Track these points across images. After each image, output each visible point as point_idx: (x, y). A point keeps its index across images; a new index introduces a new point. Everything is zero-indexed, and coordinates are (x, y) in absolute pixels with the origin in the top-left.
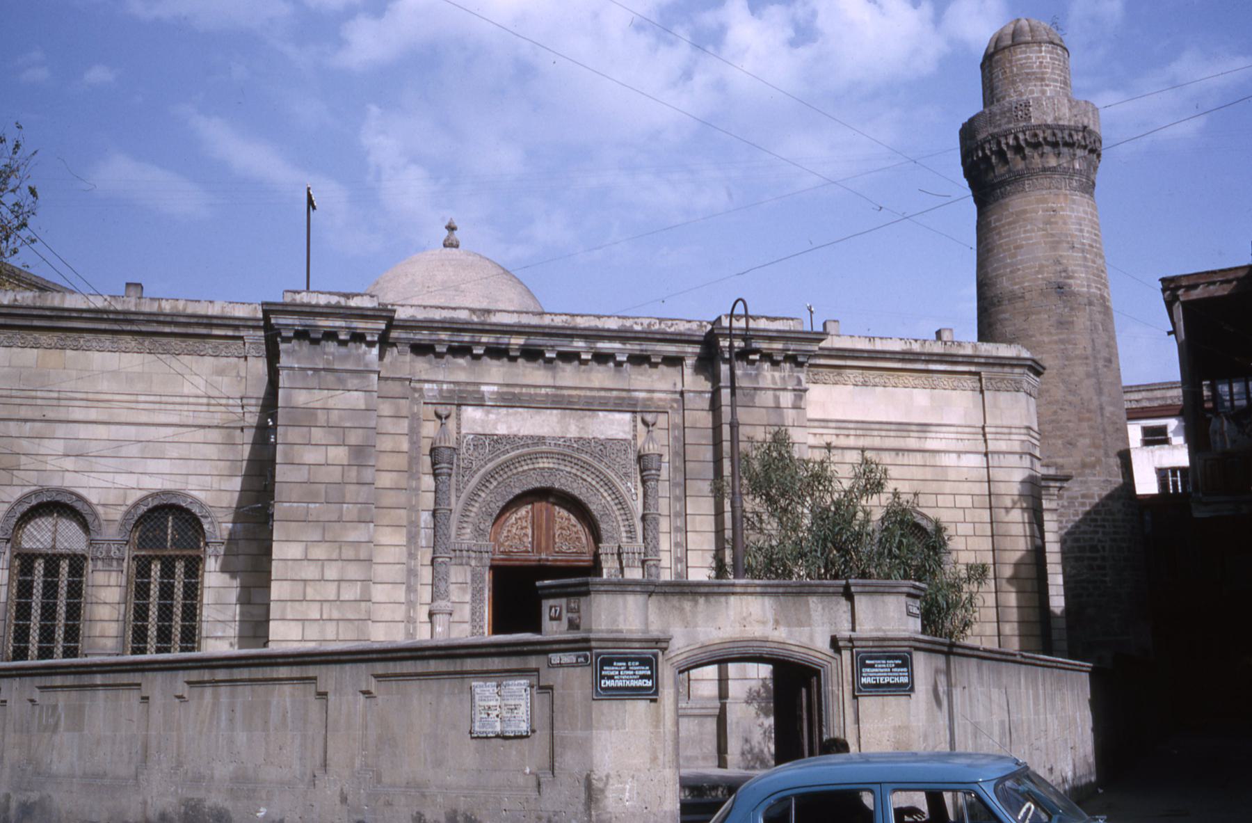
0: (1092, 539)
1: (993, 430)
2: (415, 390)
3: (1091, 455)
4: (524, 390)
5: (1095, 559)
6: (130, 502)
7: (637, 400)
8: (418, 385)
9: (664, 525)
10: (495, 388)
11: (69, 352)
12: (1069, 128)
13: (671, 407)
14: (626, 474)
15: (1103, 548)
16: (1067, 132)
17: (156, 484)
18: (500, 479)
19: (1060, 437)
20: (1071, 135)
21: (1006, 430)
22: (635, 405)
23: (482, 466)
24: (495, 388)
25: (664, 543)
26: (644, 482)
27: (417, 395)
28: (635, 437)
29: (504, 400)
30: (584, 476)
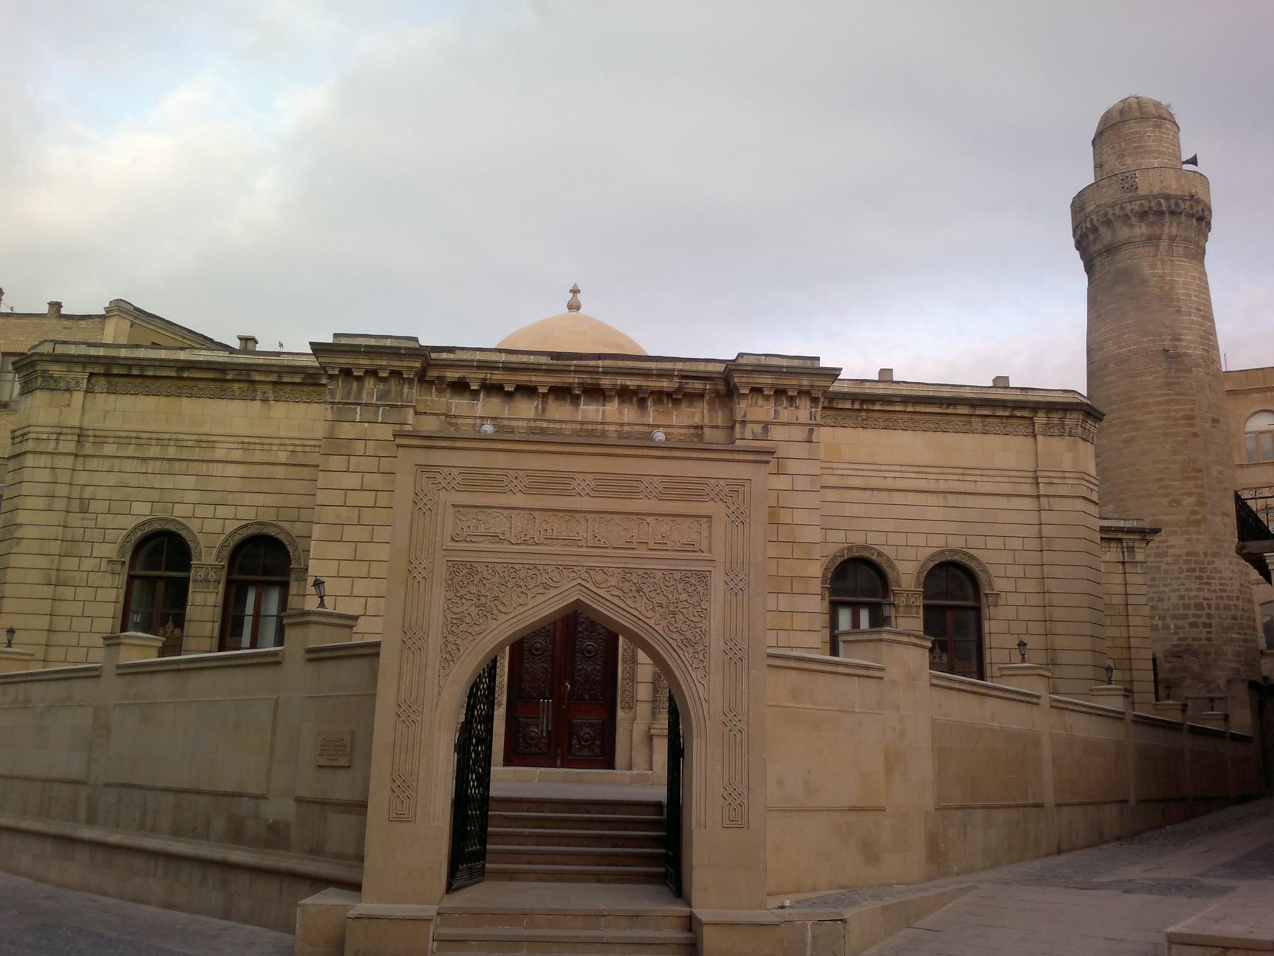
0: (1197, 597)
1: (1046, 474)
2: (451, 424)
3: (1195, 513)
4: (551, 425)
5: (1200, 616)
6: (228, 531)
8: (454, 421)
11: (185, 401)
12: (1175, 197)
15: (1209, 606)
16: (1173, 201)
17: (249, 515)
19: (1166, 495)
20: (1177, 204)
21: (1059, 474)
24: (525, 424)
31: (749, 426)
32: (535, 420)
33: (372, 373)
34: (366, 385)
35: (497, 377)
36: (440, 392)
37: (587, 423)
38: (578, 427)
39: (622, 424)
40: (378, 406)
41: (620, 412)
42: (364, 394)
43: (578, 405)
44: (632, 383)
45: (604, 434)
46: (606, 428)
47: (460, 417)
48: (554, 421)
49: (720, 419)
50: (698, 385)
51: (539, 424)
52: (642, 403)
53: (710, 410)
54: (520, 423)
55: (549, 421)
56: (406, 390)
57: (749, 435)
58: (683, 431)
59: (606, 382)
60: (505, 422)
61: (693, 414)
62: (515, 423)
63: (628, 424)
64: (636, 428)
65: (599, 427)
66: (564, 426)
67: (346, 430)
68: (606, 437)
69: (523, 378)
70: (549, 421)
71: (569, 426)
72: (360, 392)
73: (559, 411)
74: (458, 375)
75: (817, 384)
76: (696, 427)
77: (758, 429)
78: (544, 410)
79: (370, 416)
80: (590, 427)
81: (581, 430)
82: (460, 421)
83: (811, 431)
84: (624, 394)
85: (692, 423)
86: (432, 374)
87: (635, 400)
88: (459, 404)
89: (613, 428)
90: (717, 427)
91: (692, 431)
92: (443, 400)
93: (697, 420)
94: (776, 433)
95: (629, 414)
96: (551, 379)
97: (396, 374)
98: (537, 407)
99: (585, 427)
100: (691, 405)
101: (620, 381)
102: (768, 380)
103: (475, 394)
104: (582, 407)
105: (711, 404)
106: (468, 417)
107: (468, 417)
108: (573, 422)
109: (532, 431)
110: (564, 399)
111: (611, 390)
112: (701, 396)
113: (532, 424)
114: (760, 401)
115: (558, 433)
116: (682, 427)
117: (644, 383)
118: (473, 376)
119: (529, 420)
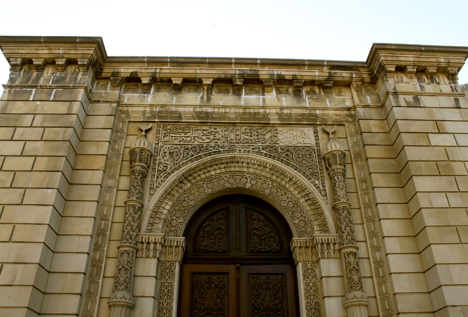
2: (122, 112)
7: (316, 116)
8: (125, 109)
9: (356, 216)
10: (191, 109)
13: (346, 121)
14: (313, 174)
18: (193, 181)
22: (315, 120)
23: (176, 169)
25: (360, 232)
26: (331, 178)
27: (123, 116)
28: (318, 145)
29: (199, 118)
30: (274, 178)
31: (401, 97)
32: (201, 106)
33: (50, 62)
34: (45, 74)
35: (166, 71)
36: (114, 87)
37: (249, 107)
38: (241, 111)
39: (282, 108)
40: (51, 88)
41: (278, 100)
42: (42, 79)
43: (239, 95)
44: (287, 73)
45: (266, 116)
46: (268, 111)
47: (132, 105)
48: (219, 107)
49: (369, 100)
50: (345, 74)
51: (204, 109)
52: (297, 93)
53: (358, 95)
54: (187, 109)
55: (214, 107)
56: (80, 76)
57: (403, 103)
58: (338, 112)
59: (264, 73)
60: (173, 109)
61: (344, 101)
62: (182, 109)
63: (287, 108)
64: (295, 111)
65: (261, 111)
66: (228, 110)
67: (20, 107)
68: (269, 119)
69: (189, 71)
70: (214, 107)
71: (233, 110)
72: (38, 78)
73: (223, 101)
74: (131, 71)
75: (452, 61)
76: (349, 109)
77: (410, 98)
78: (209, 99)
79: (44, 97)
80: (252, 111)
81: (245, 113)
82: (130, 109)
83: (457, 100)
84: (280, 83)
85: (343, 106)
86: (108, 71)
87: (291, 90)
88: (131, 97)
89: (274, 111)
90: (368, 106)
91: (345, 112)
92: (117, 92)
93: (349, 104)
94: (426, 101)
95: (287, 101)
96: (215, 72)
97: (71, 62)
98: (202, 98)
99: (248, 111)
100: (340, 94)
101: (277, 71)
102: (409, 58)
103: (146, 88)
104: (243, 96)
105: (358, 90)
106: (138, 106)
107: (138, 106)
108: (236, 107)
109: (199, 115)
110: (227, 92)
111: (267, 81)
112: (348, 85)
113: (198, 109)
114: (405, 79)
115: (224, 116)
116: (336, 110)
117: (297, 73)
118: (143, 71)
119: (195, 106)
